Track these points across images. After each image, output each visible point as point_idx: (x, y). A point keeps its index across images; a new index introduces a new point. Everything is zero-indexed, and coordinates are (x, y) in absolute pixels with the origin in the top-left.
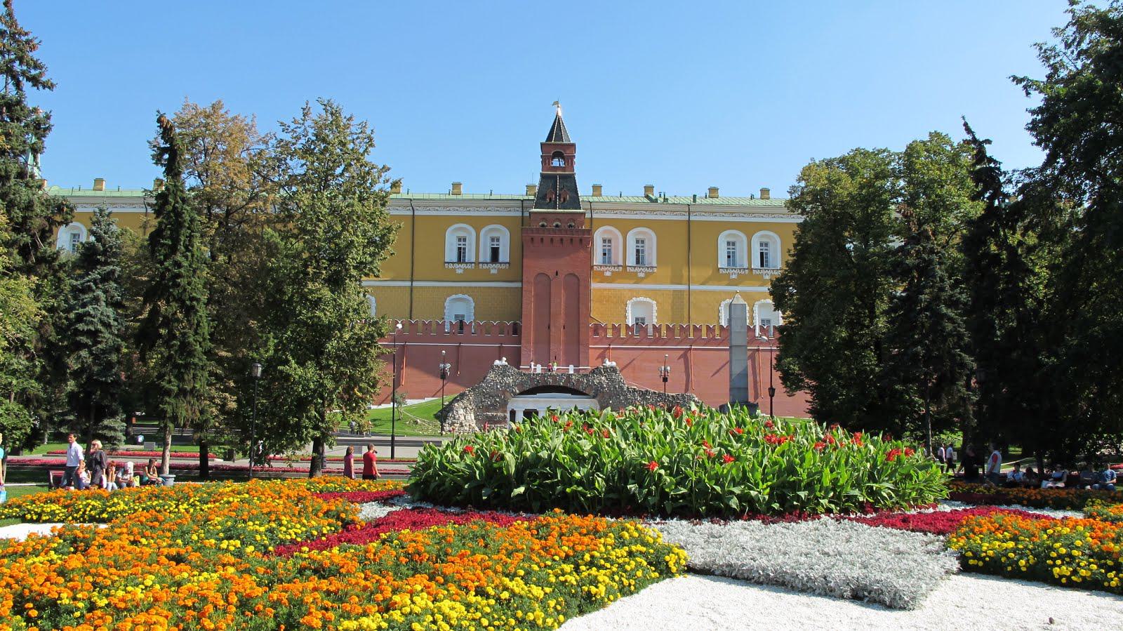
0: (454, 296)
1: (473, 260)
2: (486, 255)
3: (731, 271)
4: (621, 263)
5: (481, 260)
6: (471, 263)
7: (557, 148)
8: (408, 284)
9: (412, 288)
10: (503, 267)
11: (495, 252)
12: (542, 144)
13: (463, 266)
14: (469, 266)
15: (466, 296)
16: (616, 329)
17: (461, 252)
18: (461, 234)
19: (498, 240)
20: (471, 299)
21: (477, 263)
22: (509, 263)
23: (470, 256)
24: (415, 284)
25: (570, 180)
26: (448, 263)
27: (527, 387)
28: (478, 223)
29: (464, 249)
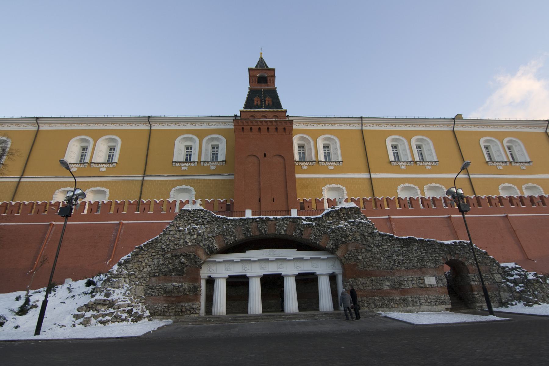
0: (178, 187)
1: (197, 160)
2: (207, 156)
3: (401, 164)
4: (314, 159)
5: (203, 159)
6: (194, 162)
9: (143, 182)
10: (221, 164)
11: (215, 156)
12: (250, 70)
13: (188, 164)
14: (193, 165)
15: (189, 187)
18: (188, 143)
19: (217, 148)
20: (193, 189)
21: (199, 162)
22: (225, 161)
23: (195, 158)
24: (146, 178)
25: (273, 94)
26: (176, 162)
27: (231, 240)
28: (201, 134)
29: (191, 155)
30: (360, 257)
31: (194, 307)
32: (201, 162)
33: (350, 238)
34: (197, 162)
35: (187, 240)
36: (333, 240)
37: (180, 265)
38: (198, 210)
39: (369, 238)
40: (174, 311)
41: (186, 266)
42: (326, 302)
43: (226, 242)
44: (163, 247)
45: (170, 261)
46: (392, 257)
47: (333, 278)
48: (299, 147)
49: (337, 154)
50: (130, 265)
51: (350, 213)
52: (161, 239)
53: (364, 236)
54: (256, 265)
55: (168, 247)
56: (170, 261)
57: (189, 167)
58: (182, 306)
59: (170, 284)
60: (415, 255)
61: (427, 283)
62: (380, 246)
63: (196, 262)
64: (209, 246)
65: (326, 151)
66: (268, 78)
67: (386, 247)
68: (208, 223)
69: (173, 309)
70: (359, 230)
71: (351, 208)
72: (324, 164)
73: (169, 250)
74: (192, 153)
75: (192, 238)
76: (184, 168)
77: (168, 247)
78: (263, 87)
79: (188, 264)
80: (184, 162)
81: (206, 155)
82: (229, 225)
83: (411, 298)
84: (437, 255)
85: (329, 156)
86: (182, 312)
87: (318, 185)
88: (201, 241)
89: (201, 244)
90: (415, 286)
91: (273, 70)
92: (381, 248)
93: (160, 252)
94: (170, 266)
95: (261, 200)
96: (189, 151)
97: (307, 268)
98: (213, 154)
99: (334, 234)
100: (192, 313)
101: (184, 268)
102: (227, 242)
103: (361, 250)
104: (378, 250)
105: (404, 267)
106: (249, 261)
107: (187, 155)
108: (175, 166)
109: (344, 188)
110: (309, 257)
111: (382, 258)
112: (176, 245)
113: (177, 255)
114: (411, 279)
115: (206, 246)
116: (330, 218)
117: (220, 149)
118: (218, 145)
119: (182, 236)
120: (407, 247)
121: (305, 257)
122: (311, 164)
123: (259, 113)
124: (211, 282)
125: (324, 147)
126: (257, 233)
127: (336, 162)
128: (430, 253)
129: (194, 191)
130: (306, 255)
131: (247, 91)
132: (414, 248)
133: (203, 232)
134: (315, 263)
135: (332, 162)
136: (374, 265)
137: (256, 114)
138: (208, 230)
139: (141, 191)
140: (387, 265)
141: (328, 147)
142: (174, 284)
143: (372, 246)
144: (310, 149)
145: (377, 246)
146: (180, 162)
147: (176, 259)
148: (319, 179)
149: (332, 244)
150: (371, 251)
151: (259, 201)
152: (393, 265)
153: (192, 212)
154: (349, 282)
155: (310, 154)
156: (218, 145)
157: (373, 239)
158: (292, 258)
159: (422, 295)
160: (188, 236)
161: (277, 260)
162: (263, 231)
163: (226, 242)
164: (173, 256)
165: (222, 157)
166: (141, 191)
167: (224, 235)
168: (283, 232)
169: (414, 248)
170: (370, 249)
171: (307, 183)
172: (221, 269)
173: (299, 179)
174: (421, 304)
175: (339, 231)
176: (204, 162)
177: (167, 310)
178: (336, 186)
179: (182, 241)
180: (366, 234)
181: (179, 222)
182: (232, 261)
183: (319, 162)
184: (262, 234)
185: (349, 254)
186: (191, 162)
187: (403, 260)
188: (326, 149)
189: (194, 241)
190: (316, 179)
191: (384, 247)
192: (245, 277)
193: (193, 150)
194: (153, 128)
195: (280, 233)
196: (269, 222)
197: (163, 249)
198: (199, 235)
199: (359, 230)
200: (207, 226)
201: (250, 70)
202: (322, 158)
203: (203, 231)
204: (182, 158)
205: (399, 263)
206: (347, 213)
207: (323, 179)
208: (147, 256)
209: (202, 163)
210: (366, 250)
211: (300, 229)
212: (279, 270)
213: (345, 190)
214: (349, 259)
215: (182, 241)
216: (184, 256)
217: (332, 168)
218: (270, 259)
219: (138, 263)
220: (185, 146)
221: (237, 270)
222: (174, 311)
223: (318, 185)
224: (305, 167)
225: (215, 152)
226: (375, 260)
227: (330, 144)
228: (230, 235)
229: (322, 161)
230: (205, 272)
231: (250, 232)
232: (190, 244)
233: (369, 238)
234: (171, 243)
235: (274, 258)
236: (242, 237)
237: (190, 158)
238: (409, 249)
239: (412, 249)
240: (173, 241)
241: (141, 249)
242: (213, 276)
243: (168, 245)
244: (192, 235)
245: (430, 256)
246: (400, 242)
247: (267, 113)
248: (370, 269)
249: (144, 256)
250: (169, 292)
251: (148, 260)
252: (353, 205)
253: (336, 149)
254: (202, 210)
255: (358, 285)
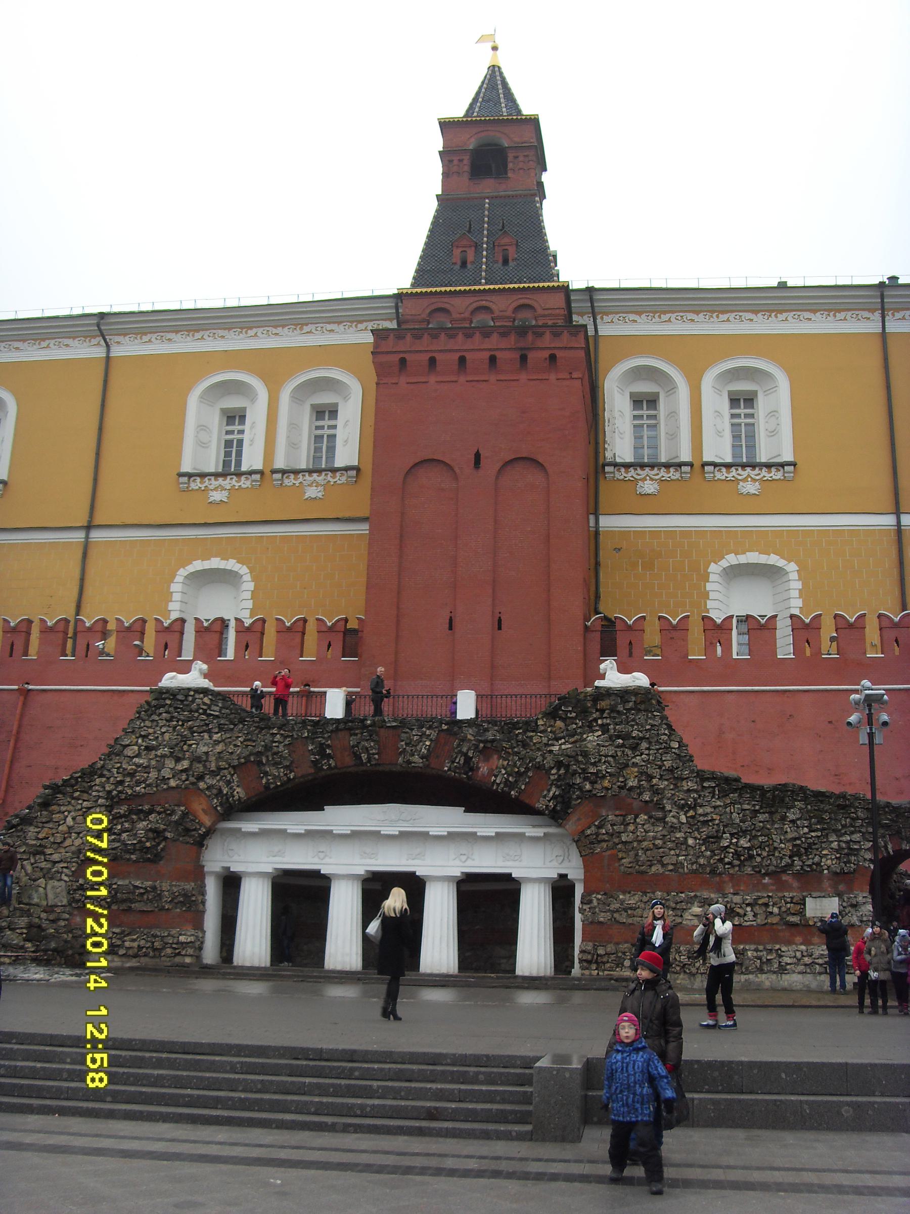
1: (258, 466)
4: (685, 457)
5: (280, 464)
6: (251, 473)
7: (494, 156)
8: (79, 536)
10: (341, 479)
12: (446, 126)
13: (227, 483)
14: (245, 483)
15: (231, 565)
16: (674, 632)
17: (232, 448)
20: (243, 570)
22: (357, 469)
23: (253, 459)
24: (96, 535)
26: (190, 476)
27: (275, 775)
29: (240, 442)
30: (624, 838)
31: (182, 939)
32: (274, 472)
33: (606, 783)
34: (261, 473)
35: (166, 773)
36: (557, 787)
37: (151, 835)
38: (198, 691)
39: (663, 784)
40: (135, 944)
41: (166, 838)
42: (533, 950)
43: (264, 781)
44: (108, 787)
45: (127, 825)
46: (718, 838)
47: (561, 892)
48: (637, 401)
49: (777, 440)
50: (32, 829)
51: (620, 708)
52: (103, 767)
53: (650, 777)
54: (346, 844)
55: (120, 788)
56: (127, 825)
57: (232, 490)
58: (155, 936)
59: (127, 882)
60: (789, 836)
61: (809, 913)
62: (690, 808)
63: (187, 831)
64: (220, 790)
65: (742, 420)
66: (510, 156)
67: (709, 810)
68: (221, 728)
69: (133, 940)
70: (637, 760)
71: (624, 694)
72: (722, 474)
73: (123, 796)
74: (246, 437)
75: (179, 767)
76: (217, 496)
77: (120, 788)
78: (488, 187)
79: (168, 835)
80: (216, 475)
81: (293, 445)
82: (274, 735)
83: (756, 950)
84: (857, 837)
85: (751, 437)
86: (155, 950)
87: (695, 553)
88: (201, 778)
89: (202, 785)
90: (775, 920)
91: (534, 122)
92: (691, 813)
93: (100, 801)
94: (124, 835)
95: (457, 624)
96: (236, 427)
97: (487, 861)
98: (318, 438)
99: (562, 771)
100: (179, 954)
101: (159, 844)
102: (268, 783)
103: (636, 817)
104: (683, 819)
105: (754, 867)
106: (326, 835)
107: (228, 444)
108: (187, 490)
109: (792, 567)
110: (491, 832)
111: (690, 841)
112: (138, 783)
113: (141, 811)
114: (765, 900)
115: (215, 791)
116: (559, 724)
117: (340, 421)
118: (336, 405)
119: (153, 763)
120: (771, 813)
121: (481, 832)
122: (673, 474)
123: (468, 300)
124: (231, 884)
125: (734, 401)
126: (349, 760)
127: (768, 466)
128: (836, 831)
129: (247, 577)
130: (487, 824)
131: (433, 205)
132: (791, 816)
133: (207, 753)
134: (512, 849)
135: (753, 466)
136: (666, 860)
137: (457, 302)
138: (219, 748)
139: (82, 580)
140: (702, 861)
141: (750, 400)
142: (138, 883)
143: (668, 807)
144: (673, 414)
145: (682, 807)
146: (203, 475)
147: (141, 820)
148: (701, 533)
149: (554, 797)
150: (663, 820)
151: (451, 628)
152: (721, 860)
153: (180, 697)
154: (590, 902)
155: (673, 436)
156: (336, 405)
157: (675, 785)
158: (443, 832)
159: (789, 943)
160: (170, 763)
161: (404, 836)
162: (364, 757)
163: (264, 781)
164: (131, 812)
165: (347, 453)
166: (82, 580)
167: (260, 763)
168: (416, 758)
169: (791, 816)
170: (660, 814)
171: (648, 552)
172: (259, 853)
173: (625, 534)
174: (782, 970)
175: (578, 761)
176: (284, 472)
177: (119, 943)
178: (762, 559)
179: (153, 775)
180: (656, 772)
181: (148, 723)
182: (282, 834)
183: (704, 465)
184: (362, 764)
185: (600, 827)
186: (239, 474)
187: (749, 849)
188: (742, 411)
189: (184, 777)
190: (686, 533)
191: (700, 811)
192: (315, 874)
193: (247, 427)
194: (116, 351)
195: (409, 762)
196: (382, 730)
197: (110, 792)
198: (196, 759)
199: (637, 760)
200: (215, 737)
201: (446, 126)
202: (717, 447)
203: (205, 749)
204: (212, 464)
205: (737, 855)
206: (613, 709)
207: (717, 533)
208: (70, 808)
209: (279, 476)
210: (650, 817)
211: (465, 755)
212: (411, 862)
213: (794, 576)
214: (600, 842)
215: (153, 775)
216: (159, 813)
217: (750, 488)
218: (385, 831)
219: (51, 825)
220: (224, 411)
221: (299, 858)
222: (135, 944)
223: (695, 553)
224: (649, 487)
225: (326, 432)
226: (670, 845)
227: (755, 393)
228: (276, 764)
229: (715, 465)
230: (218, 858)
231: (329, 756)
232: (173, 783)
233: (663, 784)
234: (128, 779)
235: (394, 831)
236: (305, 769)
237: (239, 454)
238: (777, 817)
239: (783, 818)
240: (132, 775)
241: (56, 789)
242: (234, 868)
243: (121, 783)
244: (178, 760)
245: (833, 837)
246: (753, 798)
247: (494, 298)
248: (654, 869)
249: (63, 808)
250: (124, 901)
251: (74, 819)
252: (640, 680)
253: (773, 414)
254: (205, 691)
255: (614, 912)
